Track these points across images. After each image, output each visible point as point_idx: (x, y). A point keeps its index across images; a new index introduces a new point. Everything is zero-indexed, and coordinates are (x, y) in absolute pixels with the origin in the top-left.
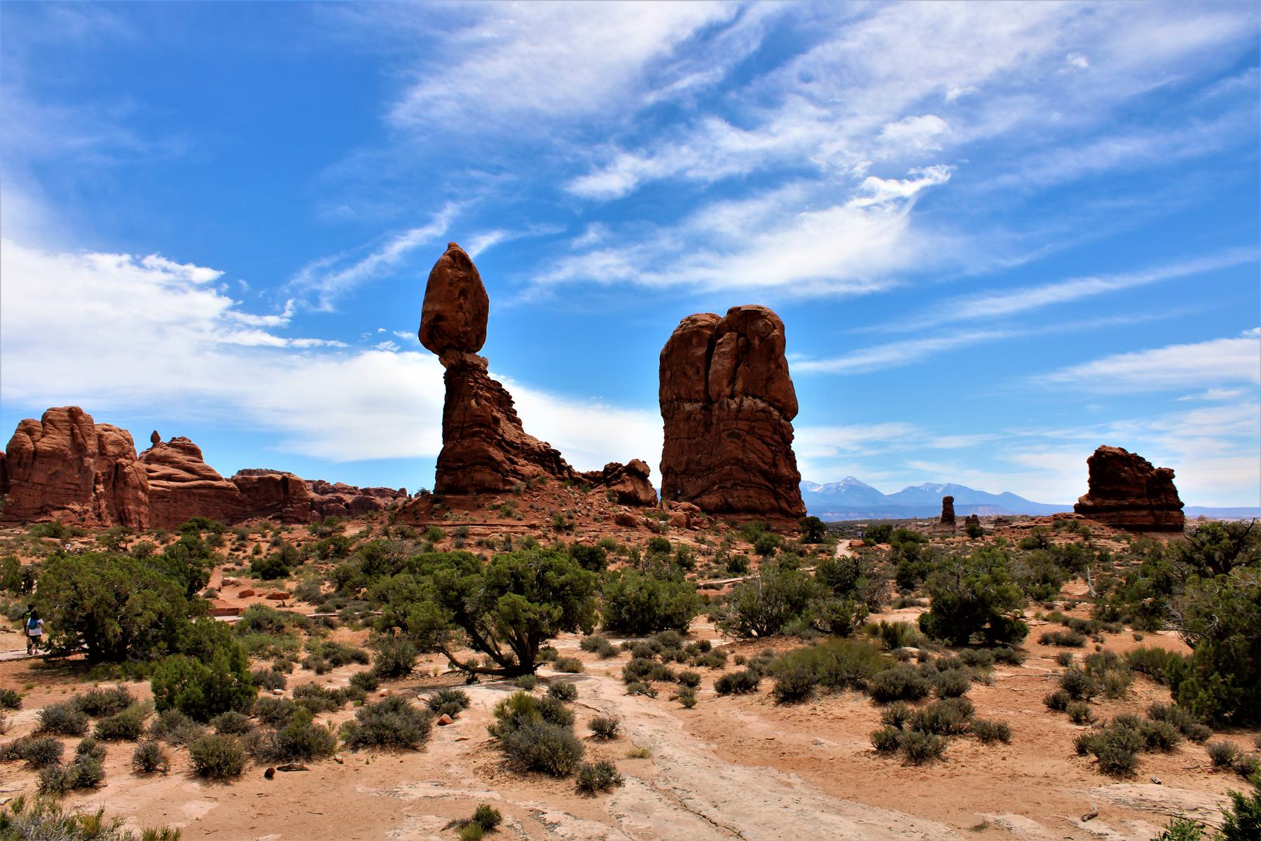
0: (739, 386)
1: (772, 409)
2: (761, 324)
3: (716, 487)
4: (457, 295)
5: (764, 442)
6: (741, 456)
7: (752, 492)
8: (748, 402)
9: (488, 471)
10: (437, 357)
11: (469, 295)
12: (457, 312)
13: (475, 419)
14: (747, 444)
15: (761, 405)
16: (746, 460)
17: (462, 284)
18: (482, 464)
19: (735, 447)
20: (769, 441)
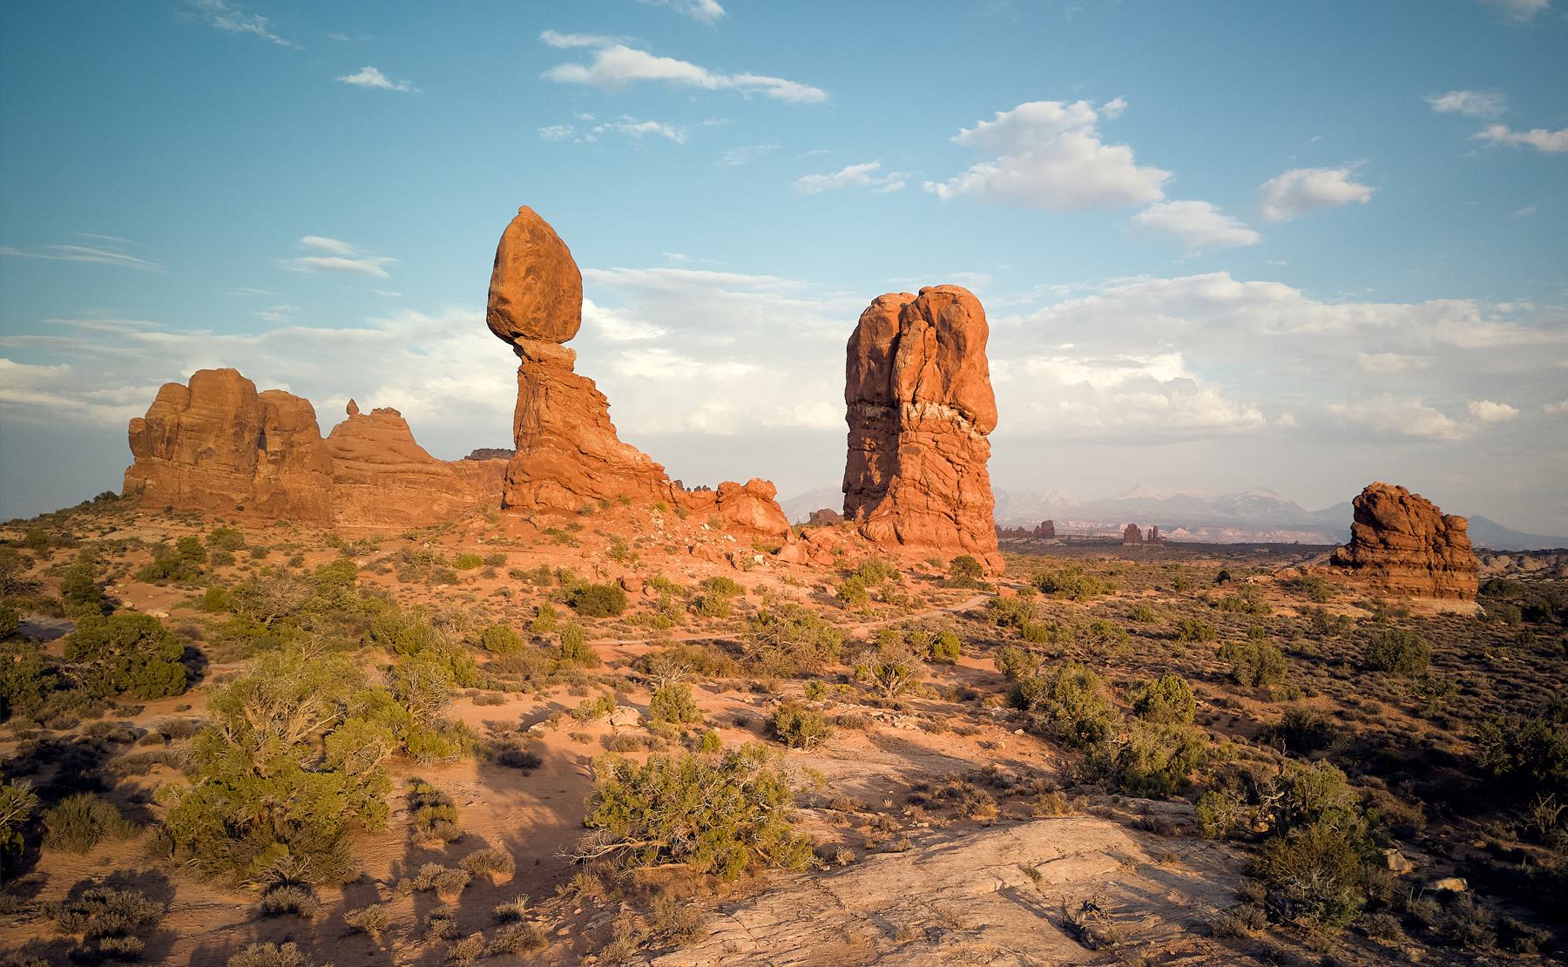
0: (922, 391)
1: (960, 418)
2: (953, 308)
3: (886, 513)
4: (523, 274)
5: (948, 460)
6: (917, 477)
7: (927, 519)
8: (932, 410)
9: (557, 487)
10: (512, 347)
11: (543, 274)
12: (524, 294)
13: (543, 424)
14: (927, 463)
15: (948, 413)
16: (924, 481)
17: (531, 260)
18: (551, 479)
19: (912, 465)
20: (953, 457)
